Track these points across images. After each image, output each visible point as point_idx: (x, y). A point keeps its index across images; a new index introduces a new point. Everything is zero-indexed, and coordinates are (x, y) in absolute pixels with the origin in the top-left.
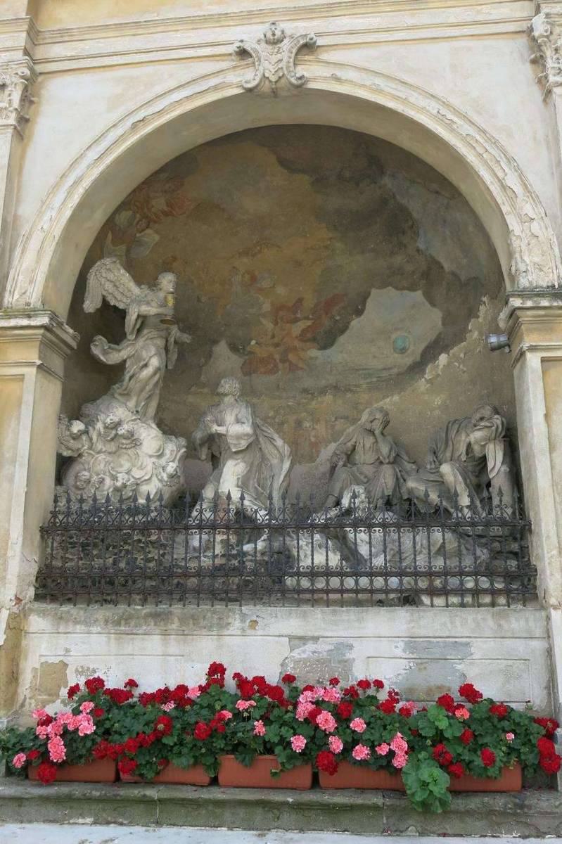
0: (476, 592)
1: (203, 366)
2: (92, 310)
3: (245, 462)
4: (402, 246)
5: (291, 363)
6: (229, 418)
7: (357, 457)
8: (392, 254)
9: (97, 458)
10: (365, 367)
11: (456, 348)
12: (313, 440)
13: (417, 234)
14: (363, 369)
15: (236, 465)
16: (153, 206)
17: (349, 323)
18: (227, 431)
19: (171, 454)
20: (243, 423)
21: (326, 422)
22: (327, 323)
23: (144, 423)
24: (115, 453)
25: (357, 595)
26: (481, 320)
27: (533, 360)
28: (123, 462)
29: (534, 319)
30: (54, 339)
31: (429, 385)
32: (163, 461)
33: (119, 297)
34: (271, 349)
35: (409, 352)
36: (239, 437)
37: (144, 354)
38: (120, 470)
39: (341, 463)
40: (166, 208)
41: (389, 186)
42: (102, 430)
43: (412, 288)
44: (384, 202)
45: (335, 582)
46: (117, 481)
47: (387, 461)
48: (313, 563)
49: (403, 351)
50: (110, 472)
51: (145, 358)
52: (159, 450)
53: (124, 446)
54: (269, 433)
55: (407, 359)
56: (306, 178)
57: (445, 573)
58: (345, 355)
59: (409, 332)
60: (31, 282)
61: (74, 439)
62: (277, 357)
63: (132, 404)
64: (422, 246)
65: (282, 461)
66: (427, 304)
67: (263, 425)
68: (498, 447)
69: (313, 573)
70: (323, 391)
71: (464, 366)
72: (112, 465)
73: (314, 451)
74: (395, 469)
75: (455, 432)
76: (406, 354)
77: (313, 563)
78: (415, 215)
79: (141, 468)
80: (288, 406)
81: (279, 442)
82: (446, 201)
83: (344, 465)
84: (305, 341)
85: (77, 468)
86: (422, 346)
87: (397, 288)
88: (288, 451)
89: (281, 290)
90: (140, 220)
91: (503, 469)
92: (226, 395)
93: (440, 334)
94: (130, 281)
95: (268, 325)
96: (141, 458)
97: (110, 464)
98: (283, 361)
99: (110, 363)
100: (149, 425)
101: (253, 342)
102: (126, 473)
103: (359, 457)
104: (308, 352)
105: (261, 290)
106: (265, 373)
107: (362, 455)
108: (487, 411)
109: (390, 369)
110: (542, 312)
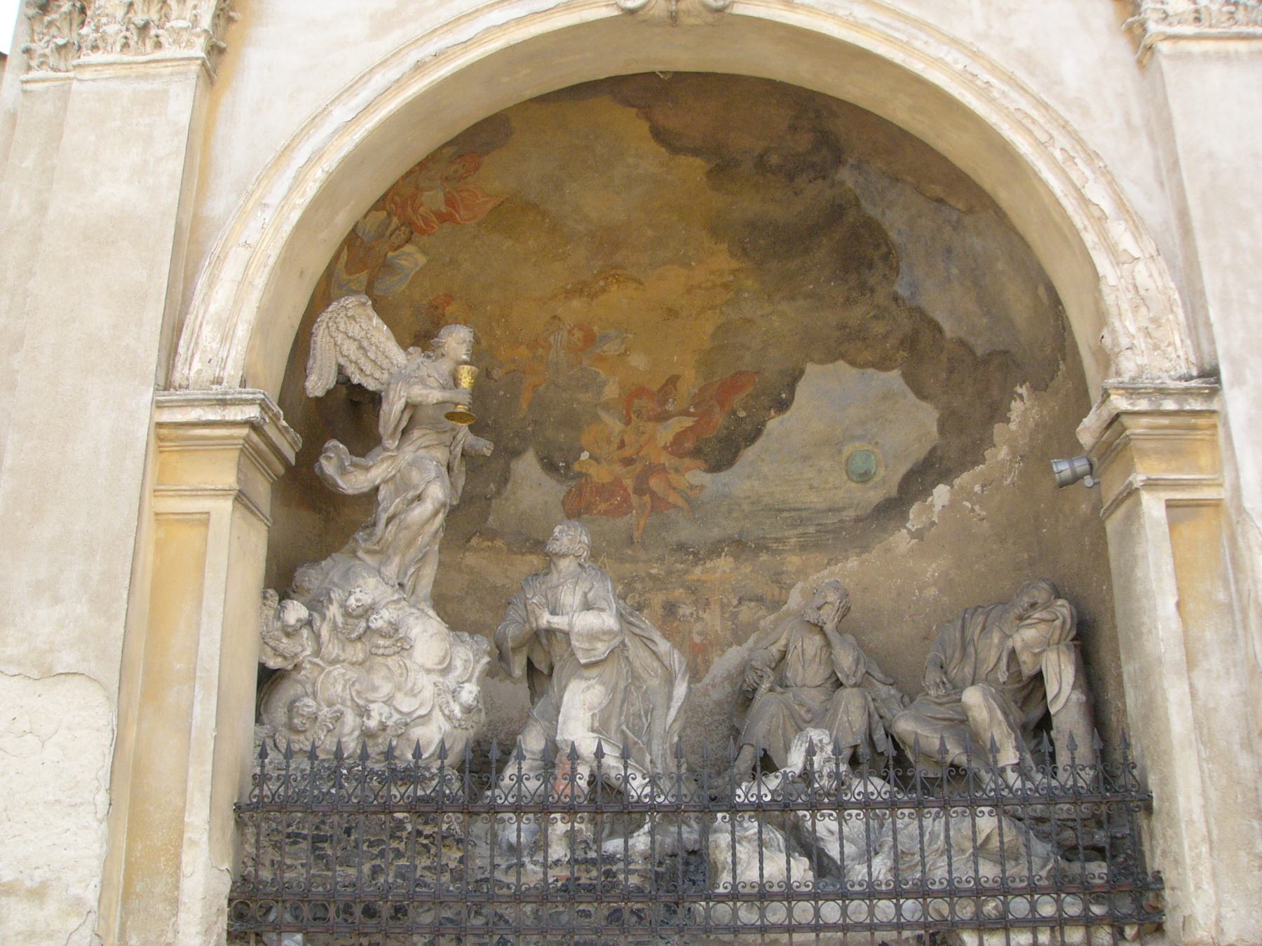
0: (1059, 923)
1: (492, 497)
2: (320, 393)
3: (603, 683)
4: (865, 288)
5: (653, 494)
6: (570, 597)
7: (789, 675)
8: (848, 302)
9: (329, 672)
10: (792, 506)
11: (965, 476)
12: (697, 639)
13: (896, 270)
14: (790, 510)
15: (588, 688)
16: (422, 204)
17: (764, 423)
18: (570, 624)
19: (465, 668)
20: (602, 610)
21: (723, 606)
22: (719, 419)
23: (414, 606)
24: (361, 664)
26: (1013, 426)
27: (1153, 506)
28: (377, 681)
30: (263, 446)
31: (914, 541)
32: (451, 681)
33: (368, 369)
34: (619, 469)
35: (876, 479)
36: (593, 636)
37: (415, 476)
38: (371, 696)
39: (765, 686)
40: (444, 209)
41: (850, 184)
42: (340, 620)
43: (883, 364)
44: (836, 213)
45: (804, 911)
46: (369, 717)
47: (852, 681)
48: (761, 876)
49: (865, 477)
50: (352, 700)
51: (411, 479)
52: (444, 658)
53: (381, 651)
54: (642, 629)
55: (872, 493)
56: (698, 161)
57: (1004, 890)
58: (756, 483)
59: (877, 443)
60: (223, 340)
61: (288, 635)
62: (629, 483)
63: (391, 570)
64: (903, 292)
65: (670, 681)
66: (911, 396)
67: (631, 615)
68: (1062, 658)
69: (763, 895)
70: (715, 550)
71: (981, 507)
72: (357, 686)
73: (699, 660)
74: (865, 698)
75: (979, 628)
76: (871, 484)
77: (761, 876)
78: (893, 235)
79: (413, 693)
80: (650, 576)
81: (663, 646)
82: (955, 217)
83: (771, 690)
84: (681, 456)
85: (292, 692)
86: (903, 469)
87: (853, 363)
88: (680, 663)
89: (638, 361)
90: (397, 228)
91: (1074, 697)
92: (564, 556)
93: (934, 449)
94: (388, 339)
95: (613, 424)
96: (412, 674)
97: (353, 684)
98: (641, 490)
99: (350, 492)
100: (422, 611)
101: (585, 456)
102: (384, 702)
103: (795, 672)
104: (687, 476)
105: (601, 359)
106: (606, 513)
107: (800, 670)
108: (1041, 595)
109: (839, 510)
110: (1165, 421)
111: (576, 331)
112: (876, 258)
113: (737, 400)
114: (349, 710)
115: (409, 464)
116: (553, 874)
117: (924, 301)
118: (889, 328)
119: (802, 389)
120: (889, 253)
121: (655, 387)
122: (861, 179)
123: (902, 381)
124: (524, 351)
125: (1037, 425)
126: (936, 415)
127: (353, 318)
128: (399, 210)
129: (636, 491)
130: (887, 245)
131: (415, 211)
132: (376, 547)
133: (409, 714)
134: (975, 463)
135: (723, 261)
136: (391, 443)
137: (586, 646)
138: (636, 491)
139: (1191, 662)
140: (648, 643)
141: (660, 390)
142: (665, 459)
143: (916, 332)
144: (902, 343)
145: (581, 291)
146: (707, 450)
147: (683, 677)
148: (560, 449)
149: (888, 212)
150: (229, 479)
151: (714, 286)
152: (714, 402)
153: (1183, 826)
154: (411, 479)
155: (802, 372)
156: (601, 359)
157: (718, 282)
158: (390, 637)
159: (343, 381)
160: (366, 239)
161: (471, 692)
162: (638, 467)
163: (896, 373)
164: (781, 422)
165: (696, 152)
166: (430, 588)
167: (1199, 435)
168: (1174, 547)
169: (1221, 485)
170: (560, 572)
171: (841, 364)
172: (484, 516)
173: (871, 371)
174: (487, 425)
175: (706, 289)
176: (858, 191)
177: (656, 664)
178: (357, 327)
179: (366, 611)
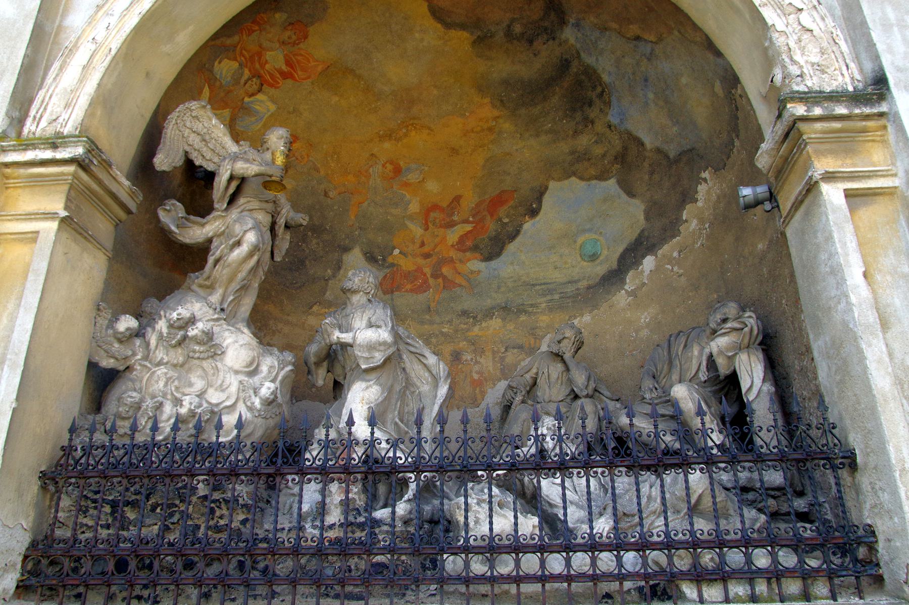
0: (775, 575)
1: (329, 279)
2: (165, 168)
3: (381, 385)
4: (588, 122)
5: (445, 278)
6: (359, 322)
7: (539, 394)
8: (576, 133)
9: (154, 372)
10: (542, 282)
11: (666, 248)
12: (476, 376)
13: (609, 104)
14: (541, 284)
15: (367, 388)
16: (266, 62)
17: (521, 226)
18: (354, 338)
19: (269, 372)
20: (379, 327)
21: (494, 353)
22: (491, 226)
23: (233, 326)
24: (182, 366)
25: (569, 585)
26: (700, 204)
27: (833, 195)
28: (194, 379)
29: (821, 136)
30: (95, 186)
31: (630, 298)
32: (256, 380)
33: (209, 155)
34: (420, 261)
35: (601, 258)
36: (371, 347)
37: (238, 229)
38: (187, 390)
39: (519, 398)
40: (284, 68)
41: (572, 41)
42: (165, 330)
43: (602, 176)
44: (564, 65)
45: (530, 563)
46: (181, 405)
47: (585, 393)
48: (491, 529)
49: (593, 257)
50: (172, 394)
51: (238, 236)
52: (251, 363)
53: (197, 355)
54: (416, 347)
55: (599, 268)
56: (465, 34)
57: (719, 543)
58: (517, 267)
59: (601, 233)
60: (67, 106)
61: (120, 341)
62: (428, 271)
63: (215, 298)
64: (614, 121)
65: (436, 386)
66: (624, 196)
67: (408, 337)
68: (753, 358)
69: (492, 548)
70: (489, 314)
71: (679, 268)
72: (176, 383)
73: (477, 391)
74: (596, 406)
75: (682, 345)
76: (598, 261)
77: (491, 529)
78: (605, 78)
79: (222, 389)
80: (442, 333)
81: (432, 360)
82: (649, 50)
83: (523, 402)
84: (464, 251)
85: (124, 387)
86: (620, 249)
87: (581, 178)
88: (444, 371)
89: (432, 186)
90: (249, 79)
91: (765, 388)
92: (355, 292)
93: (643, 231)
94: (224, 135)
95: (417, 230)
96: (221, 374)
97: (173, 382)
98: (435, 276)
99: (187, 241)
100: (239, 329)
101: (396, 252)
102: (198, 396)
103: (544, 391)
104: (468, 264)
105: (406, 185)
106: (411, 291)
107: (547, 390)
108: (731, 309)
109: (576, 282)
110: (837, 125)
111: (388, 165)
112: (594, 97)
113: (502, 211)
114: (169, 402)
115: (235, 221)
116: (331, 534)
117: (630, 126)
118: (605, 149)
119: (547, 199)
120: (603, 91)
121: (444, 204)
122: (580, 35)
123: (617, 187)
124: (351, 177)
125: (718, 198)
126: (643, 207)
127: (196, 118)
128: (249, 64)
129: (433, 276)
130: (601, 85)
131: (262, 66)
132: (206, 283)
133: (217, 405)
134: (674, 236)
135: (487, 111)
136: (220, 205)
137: (366, 355)
138: (433, 276)
139: (885, 325)
140: (421, 358)
141: (448, 206)
142: (453, 254)
143: (625, 148)
144: (616, 158)
145: (390, 136)
146: (482, 246)
147: (446, 380)
148: (379, 247)
149: (600, 59)
150: (58, 206)
151: (483, 130)
152: (486, 213)
153: (897, 474)
154: (238, 236)
155: (546, 188)
156: (406, 185)
157: (485, 126)
158: (204, 344)
159: (189, 165)
160: (224, 83)
161: (269, 388)
162: (434, 259)
163: (612, 182)
164: (533, 225)
165: (463, 27)
166: (248, 313)
167: (870, 136)
168: (856, 228)
169: (895, 175)
170: (352, 305)
171: (573, 179)
172: (323, 291)
173: (594, 182)
174: (326, 229)
175: (477, 133)
176: (578, 46)
177: (427, 374)
178: (201, 125)
179: (187, 323)
